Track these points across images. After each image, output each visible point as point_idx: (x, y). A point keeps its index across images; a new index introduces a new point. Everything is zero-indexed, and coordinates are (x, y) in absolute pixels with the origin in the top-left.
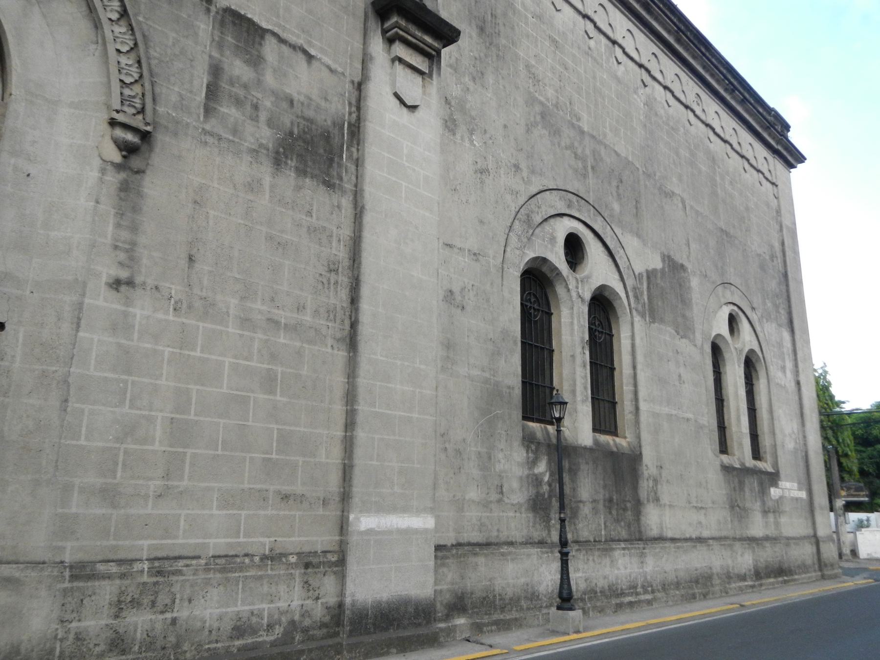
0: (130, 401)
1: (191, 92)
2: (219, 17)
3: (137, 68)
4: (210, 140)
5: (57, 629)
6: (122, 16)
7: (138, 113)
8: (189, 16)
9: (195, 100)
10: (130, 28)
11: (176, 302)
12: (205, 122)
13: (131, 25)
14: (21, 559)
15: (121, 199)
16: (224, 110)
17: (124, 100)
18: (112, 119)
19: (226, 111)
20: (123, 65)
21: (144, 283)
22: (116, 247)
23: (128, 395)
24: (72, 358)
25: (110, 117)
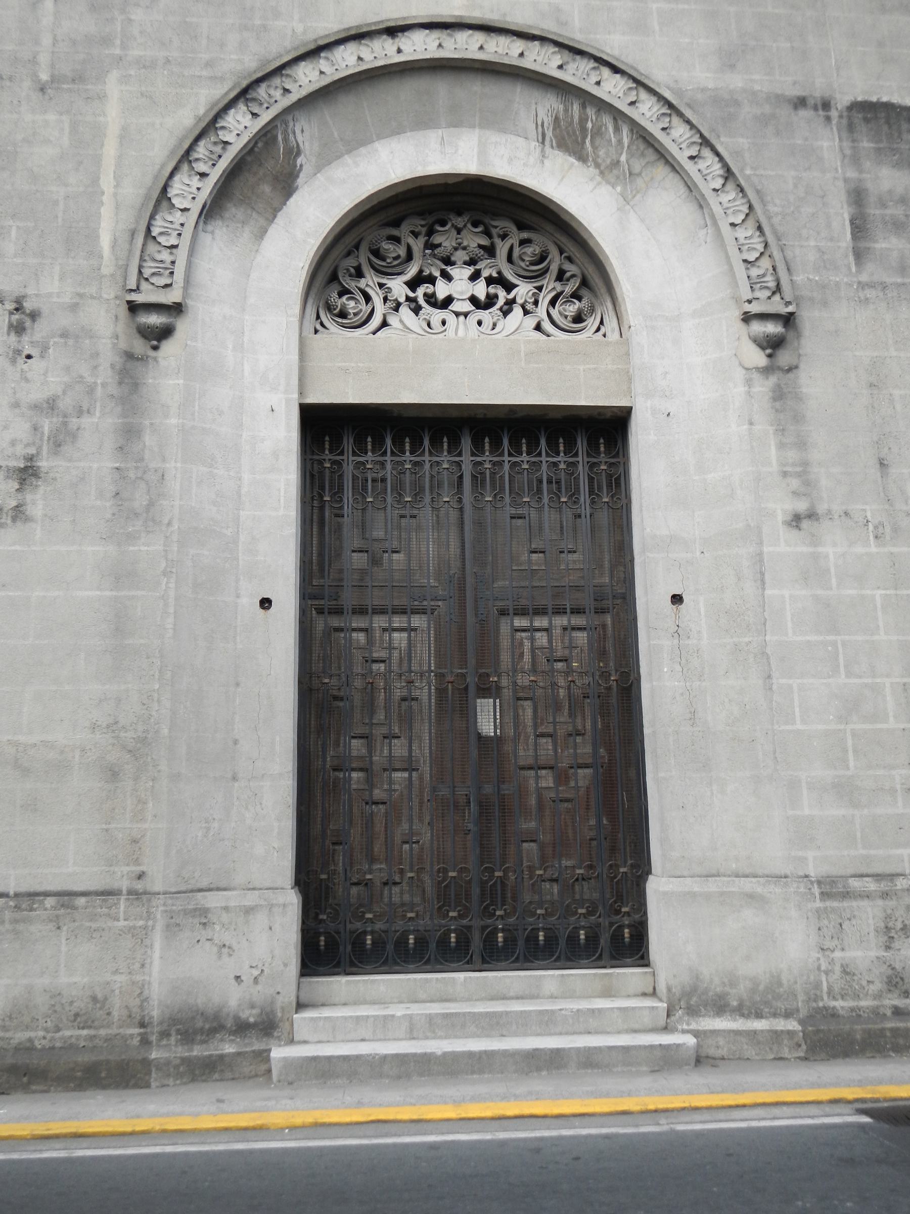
0: (846, 666)
1: (831, 240)
2: (845, 121)
3: (759, 236)
4: (870, 293)
5: (819, 959)
6: (726, 179)
7: (774, 293)
8: (806, 139)
9: (839, 247)
10: (739, 189)
11: (876, 527)
12: (859, 271)
13: (739, 186)
14: (760, 872)
15: (777, 411)
16: (880, 245)
17: (753, 284)
18: (746, 313)
19: (884, 245)
20: (742, 241)
21: (829, 512)
22: (785, 474)
23: (841, 657)
24: (765, 624)
25: (742, 313)
